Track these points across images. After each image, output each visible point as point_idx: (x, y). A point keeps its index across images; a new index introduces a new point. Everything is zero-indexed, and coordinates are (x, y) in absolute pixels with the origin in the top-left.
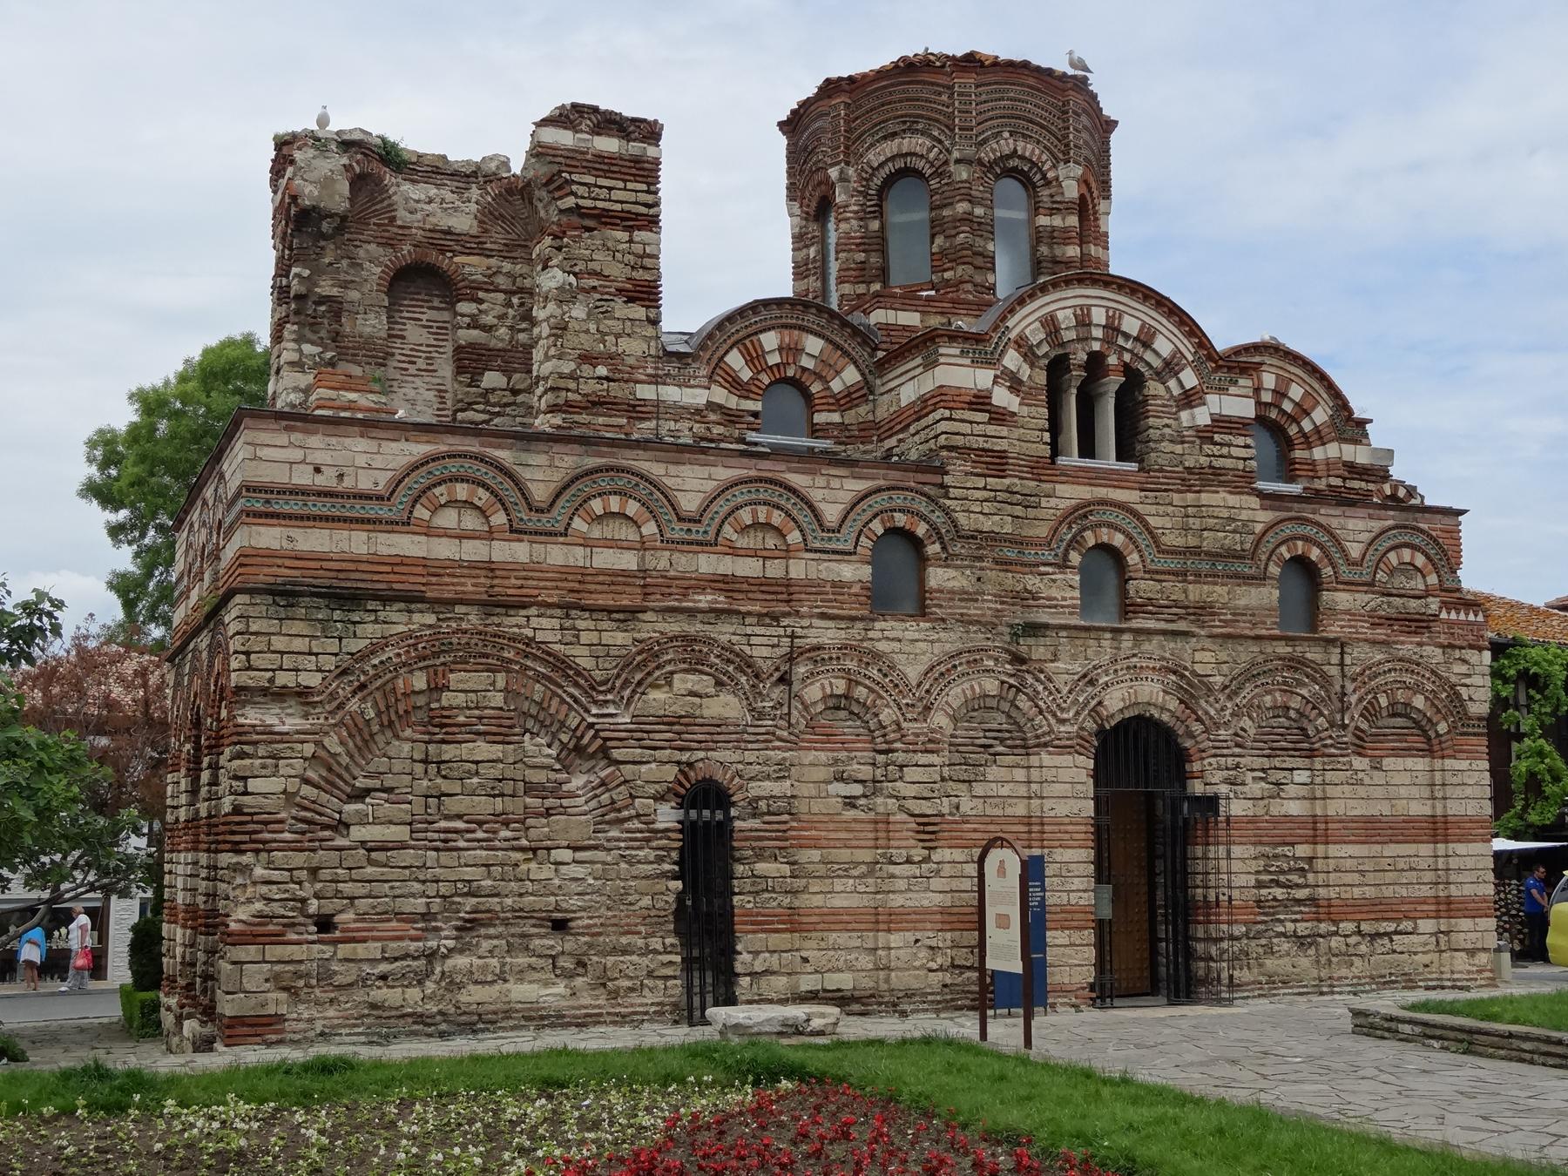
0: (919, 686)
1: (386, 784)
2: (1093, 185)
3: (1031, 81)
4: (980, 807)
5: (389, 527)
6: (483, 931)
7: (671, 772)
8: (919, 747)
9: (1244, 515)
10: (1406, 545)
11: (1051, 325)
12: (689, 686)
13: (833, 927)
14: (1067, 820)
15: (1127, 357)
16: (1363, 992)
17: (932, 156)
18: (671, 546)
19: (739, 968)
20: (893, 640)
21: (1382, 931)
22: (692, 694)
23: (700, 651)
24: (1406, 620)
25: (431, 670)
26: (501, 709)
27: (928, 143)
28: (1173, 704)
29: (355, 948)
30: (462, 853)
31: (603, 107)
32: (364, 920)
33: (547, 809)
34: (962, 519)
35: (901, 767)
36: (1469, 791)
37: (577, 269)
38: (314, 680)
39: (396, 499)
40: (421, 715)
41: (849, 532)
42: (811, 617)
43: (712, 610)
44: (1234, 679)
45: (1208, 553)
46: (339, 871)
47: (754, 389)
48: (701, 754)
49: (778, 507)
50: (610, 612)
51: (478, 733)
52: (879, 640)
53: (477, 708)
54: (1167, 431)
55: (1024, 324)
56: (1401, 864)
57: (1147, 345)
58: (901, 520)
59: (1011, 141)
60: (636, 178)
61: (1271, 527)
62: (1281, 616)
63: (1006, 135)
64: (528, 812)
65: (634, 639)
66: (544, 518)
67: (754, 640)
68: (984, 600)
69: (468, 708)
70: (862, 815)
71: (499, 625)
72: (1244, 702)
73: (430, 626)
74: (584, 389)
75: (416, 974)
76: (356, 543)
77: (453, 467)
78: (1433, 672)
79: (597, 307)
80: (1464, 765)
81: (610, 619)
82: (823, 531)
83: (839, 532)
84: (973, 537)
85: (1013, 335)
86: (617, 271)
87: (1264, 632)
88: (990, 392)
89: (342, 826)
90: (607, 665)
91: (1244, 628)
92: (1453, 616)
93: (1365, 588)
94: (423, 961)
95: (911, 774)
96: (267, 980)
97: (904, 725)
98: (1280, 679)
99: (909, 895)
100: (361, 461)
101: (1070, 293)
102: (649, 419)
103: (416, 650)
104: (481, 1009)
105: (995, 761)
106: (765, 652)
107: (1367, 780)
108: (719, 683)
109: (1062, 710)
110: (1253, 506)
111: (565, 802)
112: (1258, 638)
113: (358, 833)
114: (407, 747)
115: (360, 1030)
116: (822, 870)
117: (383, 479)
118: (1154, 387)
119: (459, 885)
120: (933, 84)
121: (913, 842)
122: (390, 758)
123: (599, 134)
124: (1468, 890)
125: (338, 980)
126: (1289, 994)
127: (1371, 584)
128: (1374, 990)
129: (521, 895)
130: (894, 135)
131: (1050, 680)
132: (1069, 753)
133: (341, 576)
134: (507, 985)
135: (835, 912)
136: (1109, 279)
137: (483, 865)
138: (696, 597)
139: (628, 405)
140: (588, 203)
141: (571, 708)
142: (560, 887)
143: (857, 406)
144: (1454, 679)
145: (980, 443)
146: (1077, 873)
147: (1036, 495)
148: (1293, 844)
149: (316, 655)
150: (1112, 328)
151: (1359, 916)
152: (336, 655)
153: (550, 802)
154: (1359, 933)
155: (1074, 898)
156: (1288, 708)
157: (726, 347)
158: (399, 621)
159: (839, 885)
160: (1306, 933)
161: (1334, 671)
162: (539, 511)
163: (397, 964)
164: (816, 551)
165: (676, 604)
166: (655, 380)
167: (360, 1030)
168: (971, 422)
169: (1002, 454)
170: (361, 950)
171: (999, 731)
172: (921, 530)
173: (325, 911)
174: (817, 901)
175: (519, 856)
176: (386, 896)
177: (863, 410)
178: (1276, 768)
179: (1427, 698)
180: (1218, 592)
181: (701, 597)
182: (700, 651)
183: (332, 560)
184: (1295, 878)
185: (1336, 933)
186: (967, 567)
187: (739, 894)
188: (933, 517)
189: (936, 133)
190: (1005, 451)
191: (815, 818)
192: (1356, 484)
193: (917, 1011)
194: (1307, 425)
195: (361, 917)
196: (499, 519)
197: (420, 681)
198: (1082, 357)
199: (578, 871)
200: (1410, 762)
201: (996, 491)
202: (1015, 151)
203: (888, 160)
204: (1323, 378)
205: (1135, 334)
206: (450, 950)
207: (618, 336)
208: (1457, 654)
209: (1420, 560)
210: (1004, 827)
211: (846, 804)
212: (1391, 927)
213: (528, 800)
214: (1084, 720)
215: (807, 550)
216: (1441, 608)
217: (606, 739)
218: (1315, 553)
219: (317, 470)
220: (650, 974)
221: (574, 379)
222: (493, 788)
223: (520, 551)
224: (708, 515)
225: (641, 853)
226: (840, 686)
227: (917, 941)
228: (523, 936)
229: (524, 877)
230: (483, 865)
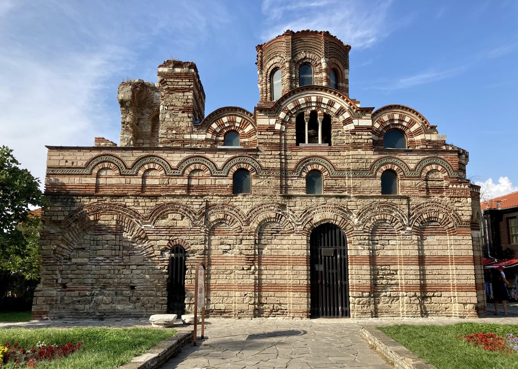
0: (248, 215)
1: (83, 247)
4: (270, 252)
5: (85, 176)
6: (108, 289)
8: (247, 234)
9: (367, 157)
10: (435, 163)
14: (299, 257)
15: (325, 111)
18: (169, 177)
20: (240, 201)
22: (174, 219)
23: (177, 207)
24: (435, 189)
25: (95, 215)
27: (280, 58)
28: (339, 219)
30: (102, 266)
32: (74, 285)
34: (263, 164)
35: (241, 240)
36: (462, 247)
37: (167, 105)
38: (62, 218)
40: (93, 227)
41: (226, 170)
42: (213, 196)
43: (180, 195)
45: (353, 170)
46: (68, 271)
48: (176, 237)
49: (203, 164)
51: (109, 232)
52: (235, 202)
54: (340, 132)
56: (435, 272)
58: (243, 166)
59: (304, 54)
60: (185, 78)
62: (382, 189)
63: (303, 52)
65: (156, 204)
66: (130, 171)
67: (194, 203)
70: (230, 255)
71: (115, 201)
73: (95, 203)
74: (169, 137)
75: (88, 300)
77: (104, 158)
80: (461, 238)
81: (149, 199)
84: (266, 170)
85: (283, 108)
86: (179, 104)
89: (70, 259)
90: (147, 212)
91: (367, 194)
92: (455, 186)
94: (90, 297)
95: (244, 242)
96: (44, 302)
97: (243, 227)
100: (78, 158)
101: (304, 93)
102: (188, 144)
105: (275, 238)
106: (198, 206)
108: (183, 217)
110: (371, 154)
111: (135, 252)
112: (372, 197)
113: (74, 260)
114: (89, 236)
115: (71, 316)
117: (84, 163)
118: (334, 119)
119: (100, 275)
120: (280, 41)
125: (66, 302)
129: (121, 279)
130: (272, 58)
136: (317, 87)
138: (176, 191)
140: (172, 87)
143: (252, 136)
145: (270, 141)
146: (302, 274)
147: (290, 156)
148: (389, 265)
149: (63, 211)
150: (319, 102)
151: (416, 290)
152: (69, 211)
153: (130, 252)
155: (302, 282)
156: (386, 220)
167: (71, 316)
170: (73, 294)
171: (277, 229)
172: (249, 169)
173: (63, 282)
175: (120, 267)
177: (253, 137)
178: (382, 240)
180: (358, 182)
182: (177, 207)
183: (69, 186)
184: (390, 277)
185: (406, 296)
187: (187, 279)
188: (253, 165)
189: (282, 55)
193: (245, 317)
194: (412, 129)
198: (309, 112)
201: (275, 155)
202: (306, 57)
203: (271, 66)
205: (327, 103)
206: (97, 294)
207: (179, 122)
208: (456, 199)
209: (440, 168)
211: (223, 252)
212: (431, 294)
213: (124, 251)
215: (212, 176)
218: (396, 168)
220: (157, 303)
222: (112, 248)
223: (123, 180)
226: (221, 216)
228: (121, 290)
229: (121, 273)
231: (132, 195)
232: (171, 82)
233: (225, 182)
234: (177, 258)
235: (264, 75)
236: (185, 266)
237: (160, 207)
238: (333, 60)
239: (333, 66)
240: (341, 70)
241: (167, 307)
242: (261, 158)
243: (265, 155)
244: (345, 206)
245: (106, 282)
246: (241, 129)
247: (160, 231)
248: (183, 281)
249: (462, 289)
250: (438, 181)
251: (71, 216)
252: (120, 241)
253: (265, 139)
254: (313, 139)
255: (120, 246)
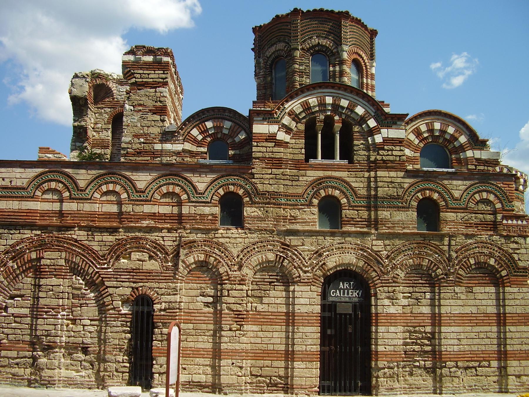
2: (363, 55)
3: (326, 16)
7: (128, 291)
8: (237, 282)
9: (399, 180)
11: (306, 107)
12: (137, 257)
13: (197, 356)
16: (457, 393)
17: (285, 49)
18: (132, 202)
19: (154, 370)
21: (471, 365)
23: (143, 243)
26: (63, 266)
29: (7, 353)
30: (46, 320)
31: (146, 46)
33: (81, 304)
34: (260, 187)
36: (518, 302)
37: (134, 104)
39: (29, 189)
44: (393, 252)
47: (204, 143)
48: (142, 284)
50: (108, 228)
51: (55, 275)
52: (220, 238)
53: (54, 265)
55: (293, 106)
56: (482, 335)
57: (352, 111)
58: (232, 188)
61: (412, 185)
64: (74, 306)
65: (116, 239)
68: (268, 221)
69: (51, 265)
72: (398, 262)
73: (38, 235)
74: (135, 147)
76: (14, 205)
77: (50, 176)
78: (499, 248)
79: (141, 117)
80: (516, 290)
82: (197, 194)
83: (204, 194)
85: (287, 111)
86: (150, 103)
87: (408, 231)
88: (276, 134)
89: (6, 309)
91: (398, 230)
93: (462, 211)
97: (230, 273)
98: (417, 252)
99: (229, 344)
100: (18, 176)
103: (33, 244)
104: (50, 379)
105: (274, 289)
106: (170, 243)
107: (463, 297)
108: (151, 257)
109: (306, 267)
113: (11, 310)
114: (29, 279)
115: (7, 382)
116: (193, 332)
117: (25, 181)
118: (356, 129)
119: (44, 332)
121: (231, 322)
122: (23, 284)
123: (145, 55)
124: (516, 347)
126: (420, 393)
127: (466, 209)
128: (465, 393)
130: (274, 44)
131: (300, 254)
132: (309, 286)
133: (8, 217)
134: (61, 371)
135: (198, 350)
137: (53, 325)
138: (142, 222)
139: (151, 152)
140: (140, 80)
141: (90, 266)
142: (84, 335)
144: (511, 251)
145: (271, 155)
146: (310, 337)
147: (297, 176)
148: (424, 326)
151: (457, 359)
153: (81, 302)
154: (457, 367)
157: (191, 128)
158: (28, 234)
159: (200, 339)
160: (430, 366)
161: (446, 248)
162: (81, 191)
163: (22, 359)
164: (193, 202)
165: (134, 225)
166: (162, 141)
168: (266, 147)
169: (280, 159)
170: (10, 354)
172: (241, 192)
174: (191, 344)
176: (19, 334)
179: (496, 261)
181: (144, 222)
185: (445, 367)
186: (261, 207)
187: (155, 340)
188: (247, 187)
190: (281, 158)
191: (190, 311)
192: (482, 168)
193: (232, 393)
195: (10, 341)
196: (66, 194)
197: (34, 256)
198: (322, 117)
199: (92, 329)
200: (487, 289)
201: (276, 175)
202: (319, 43)
203: (272, 53)
204: (464, 124)
205: (346, 106)
207: (148, 127)
208: (512, 239)
210: (278, 317)
211: (204, 305)
214: (316, 271)
215: (189, 202)
216: (503, 219)
217: (103, 278)
218: (436, 196)
219: (3, 180)
220: (117, 371)
221: (131, 144)
224: (148, 190)
225: (114, 323)
226: (202, 257)
227: (233, 364)
230: (53, 325)
231: (85, 227)
232: (140, 74)
233: (207, 210)
234: (142, 312)
235: (262, 65)
236: (153, 323)
237: (120, 244)
238: (356, 50)
239: (355, 56)
240: (364, 62)
241: (129, 376)
242: (257, 179)
243: (263, 174)
244: (370, 247)
245: (52, 341)
246: (232, 137)
247: (120, 275)
248: (150, 343)
249: (516, 357)
250: (490, 214)
251: (7, 253)
252: (68, 287)
253: (262, 152)
254: (328, 154)
255: (68, 293)
